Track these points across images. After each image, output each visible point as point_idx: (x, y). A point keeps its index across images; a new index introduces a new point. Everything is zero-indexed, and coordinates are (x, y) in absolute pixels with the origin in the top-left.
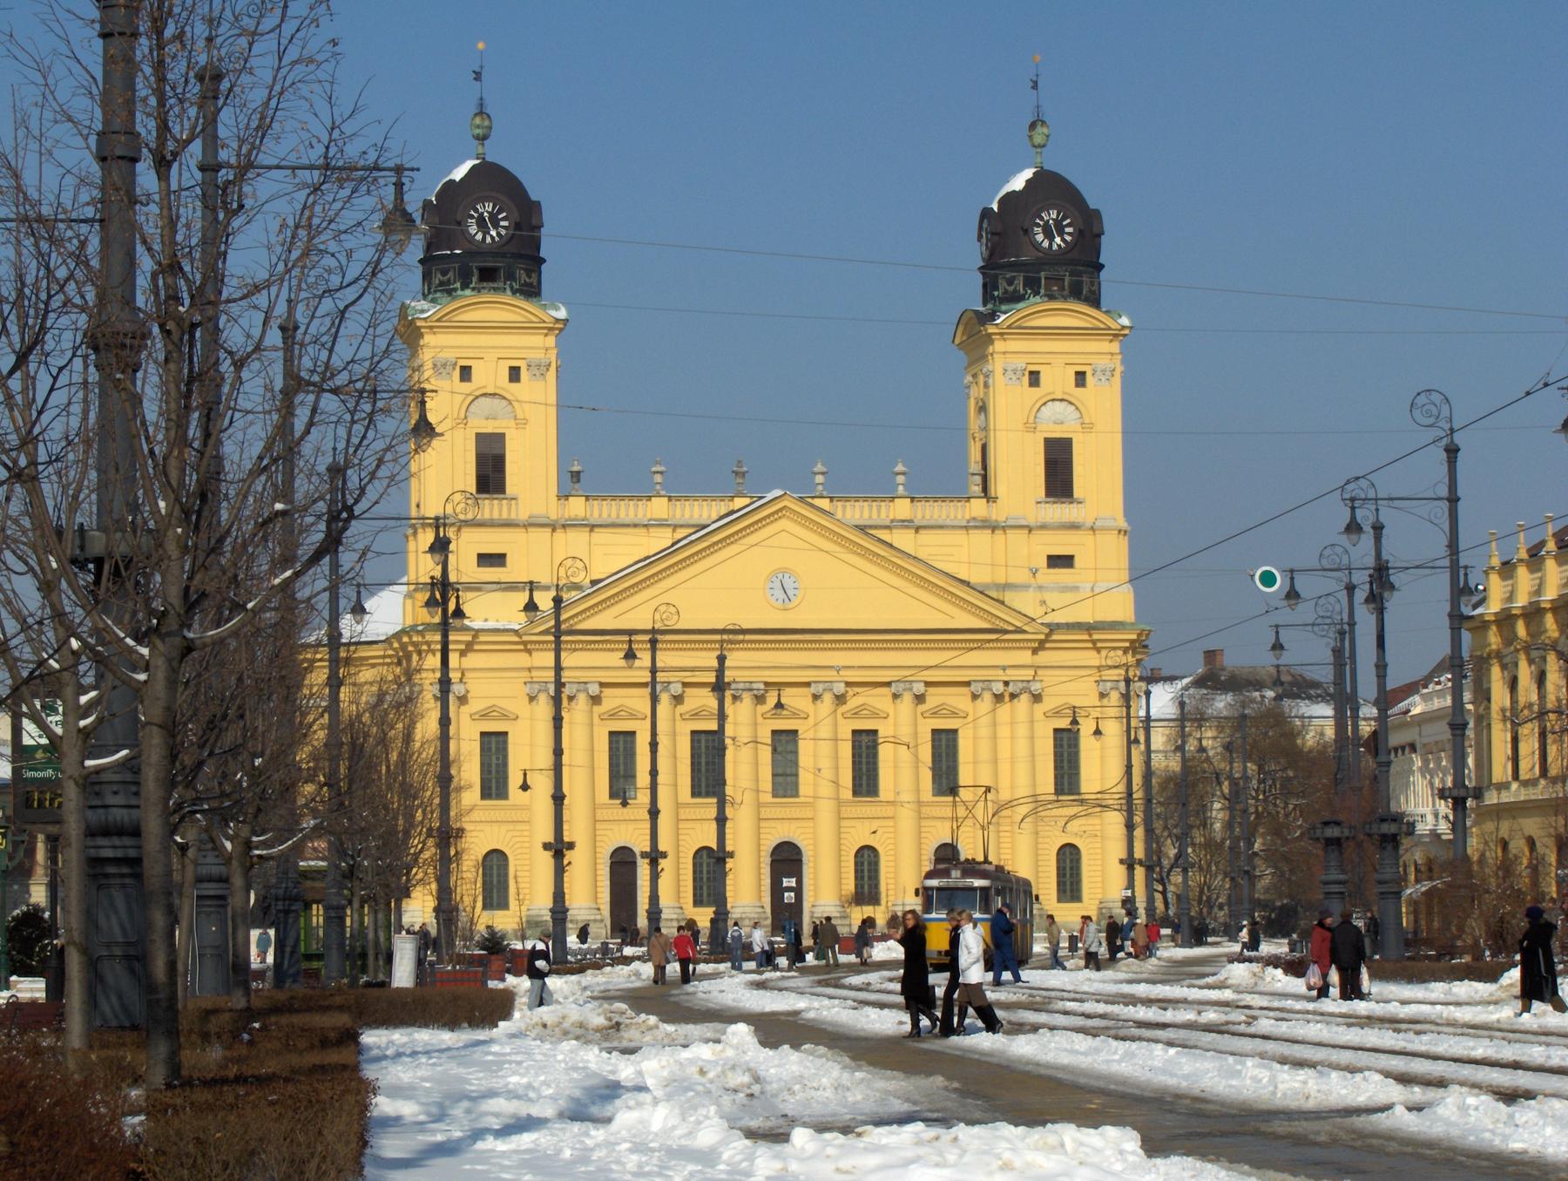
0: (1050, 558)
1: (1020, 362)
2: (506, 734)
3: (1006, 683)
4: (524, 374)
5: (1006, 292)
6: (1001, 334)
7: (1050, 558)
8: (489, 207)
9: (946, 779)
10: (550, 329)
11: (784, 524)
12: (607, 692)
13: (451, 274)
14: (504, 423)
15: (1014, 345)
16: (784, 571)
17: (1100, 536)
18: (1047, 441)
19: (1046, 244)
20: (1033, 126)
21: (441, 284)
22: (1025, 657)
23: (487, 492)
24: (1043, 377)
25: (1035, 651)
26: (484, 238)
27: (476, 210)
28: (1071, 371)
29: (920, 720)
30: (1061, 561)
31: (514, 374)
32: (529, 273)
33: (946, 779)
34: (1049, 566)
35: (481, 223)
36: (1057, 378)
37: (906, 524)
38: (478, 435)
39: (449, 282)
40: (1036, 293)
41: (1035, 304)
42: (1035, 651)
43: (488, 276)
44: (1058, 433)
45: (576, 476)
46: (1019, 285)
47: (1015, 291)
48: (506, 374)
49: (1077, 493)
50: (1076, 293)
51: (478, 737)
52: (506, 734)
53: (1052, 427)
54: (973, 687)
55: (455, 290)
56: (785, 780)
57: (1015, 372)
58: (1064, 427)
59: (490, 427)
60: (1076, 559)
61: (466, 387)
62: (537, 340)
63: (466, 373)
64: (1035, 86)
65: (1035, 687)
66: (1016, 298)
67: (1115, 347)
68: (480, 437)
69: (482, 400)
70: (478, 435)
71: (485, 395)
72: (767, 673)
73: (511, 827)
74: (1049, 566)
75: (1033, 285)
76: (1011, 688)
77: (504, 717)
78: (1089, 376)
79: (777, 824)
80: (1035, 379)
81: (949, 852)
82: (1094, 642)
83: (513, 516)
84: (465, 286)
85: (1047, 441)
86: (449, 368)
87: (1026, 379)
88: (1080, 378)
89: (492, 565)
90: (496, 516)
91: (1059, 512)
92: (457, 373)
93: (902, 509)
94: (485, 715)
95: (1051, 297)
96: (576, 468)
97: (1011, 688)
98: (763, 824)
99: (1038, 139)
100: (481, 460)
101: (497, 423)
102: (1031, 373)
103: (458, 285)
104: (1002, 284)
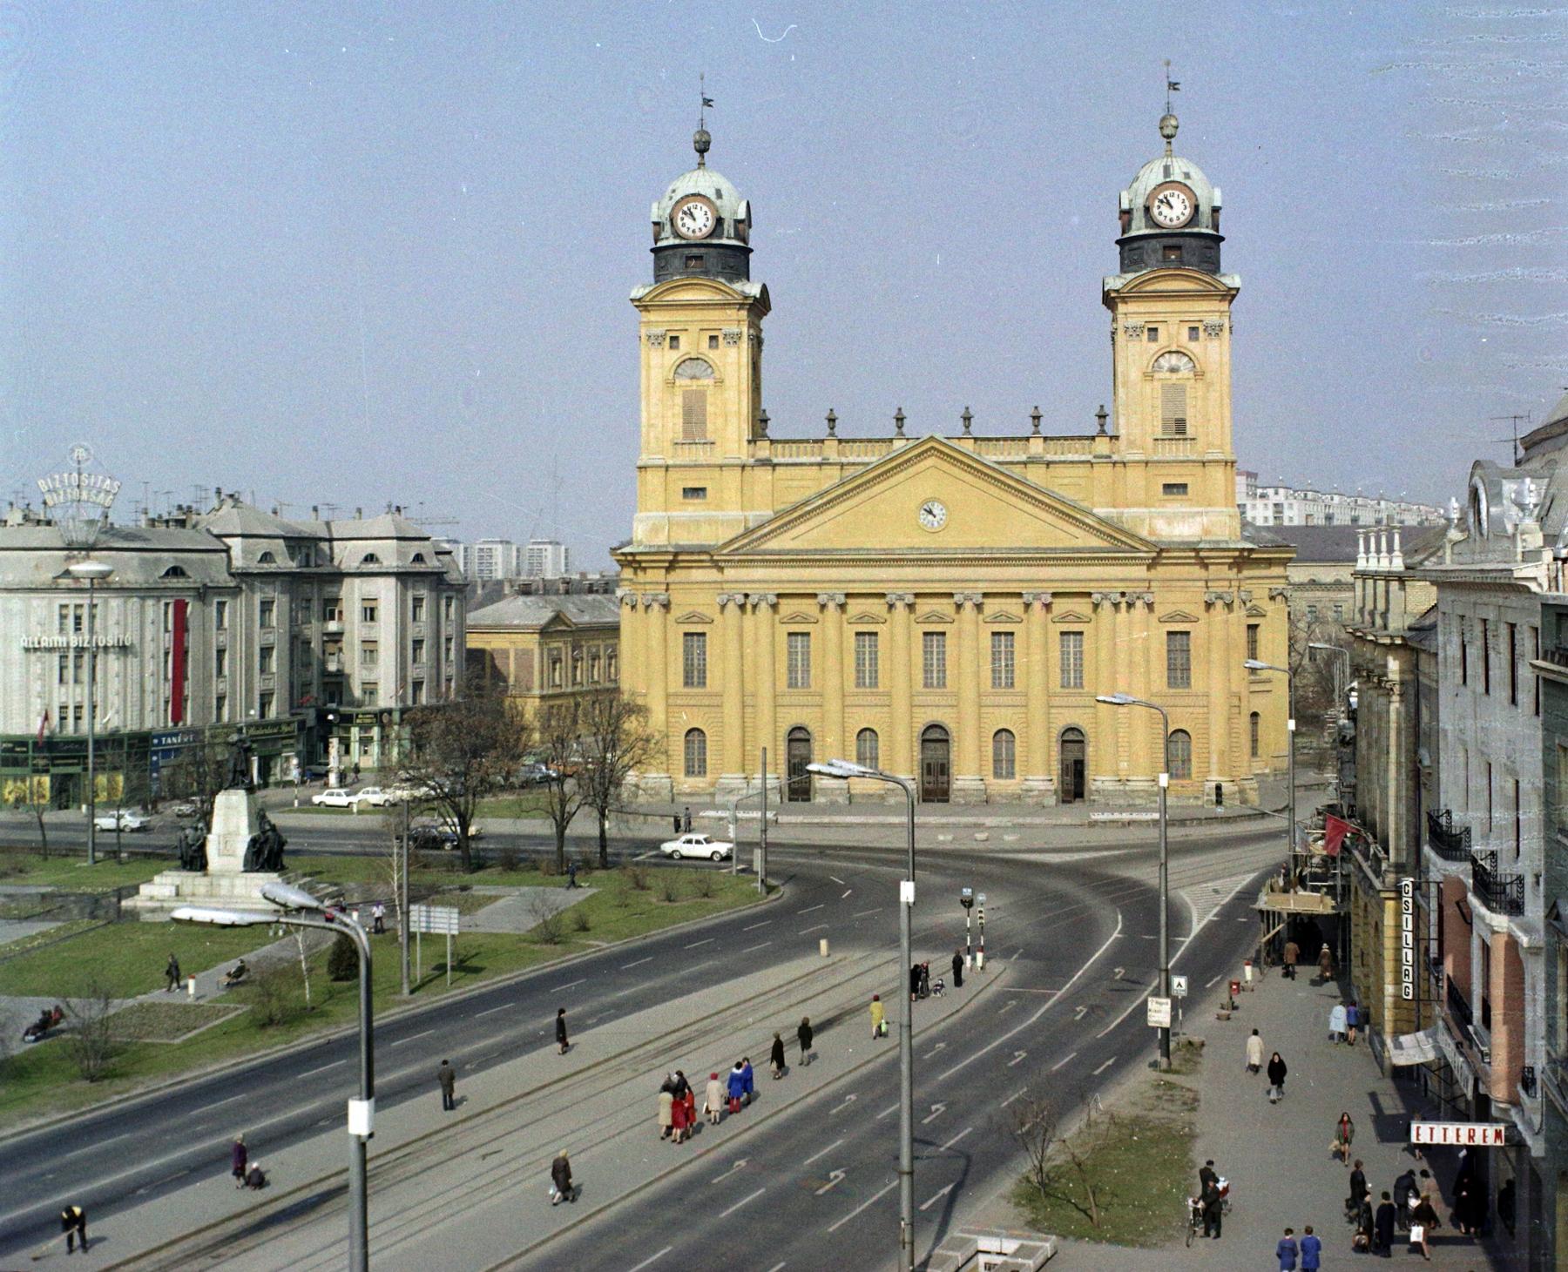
3: (1123, 594)
11: (931, 461)
12: (783, 601)
15: (1132, 307)
17: (1210, 469)
20: (1163, 119)
22: (1140, 572)
25: (1150, 567)
29: (1051, 625)
36: (1174, 333)
42: (1150, 567)
53: (1168, 375)
54: (956, 598)
57: (1135, 328)
58: (1180, 375)
59: (694, 385)
62: (732, 313)
65: (1148, 598)
67: (1224, 306)
76: (1119, 599)
78: (1201, 334)
87: (1145, 336)
97: (1119, 599)
98: (915, 710)
99: (1168, 131)
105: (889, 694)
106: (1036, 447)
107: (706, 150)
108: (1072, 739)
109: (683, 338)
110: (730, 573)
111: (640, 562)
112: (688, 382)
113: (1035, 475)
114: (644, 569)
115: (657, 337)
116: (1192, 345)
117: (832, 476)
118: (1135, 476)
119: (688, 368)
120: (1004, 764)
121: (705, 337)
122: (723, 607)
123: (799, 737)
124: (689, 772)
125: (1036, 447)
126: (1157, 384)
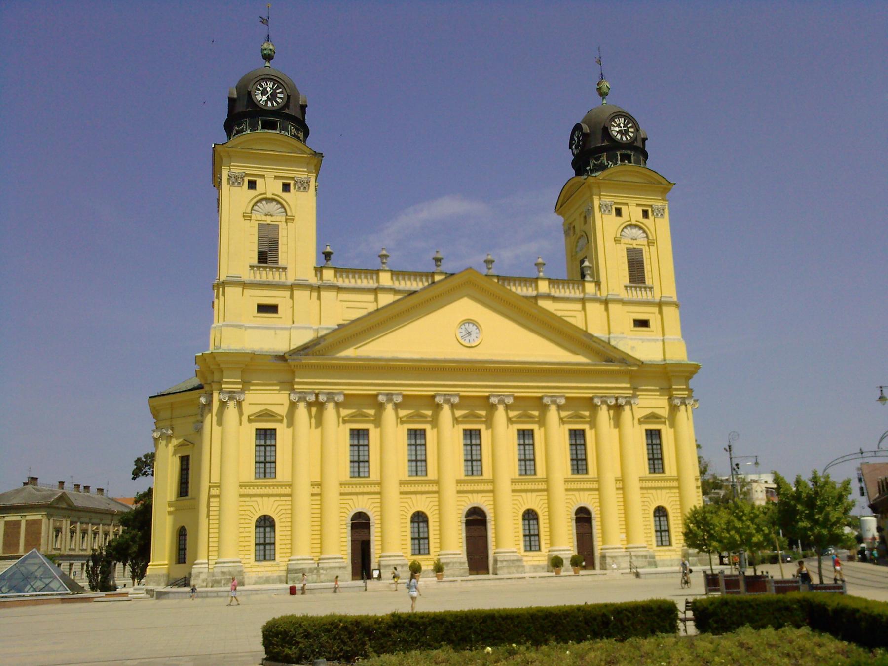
2: (275, 430)
13: (244, 126)
16: (469, 321)
18: (628, 250)
19: (619, 136)
24: (624, 209)
27: (262, 86)
30: (643, 323)
31: (286, 187)
32: (297, 130)
33: (579, 463)
36: (632, 212)
43: (269, 125)
45: (327, 255)
46: (604, 159)
49: (648, 282)
50: (638, 162)
52: (275, 430)
53: (631, 241)
59: (269, 220)
60: (651, 323)
61: (252, 193)
63: (252, 185)
64: (599, 62)
66: (603, 168)
68: (261, 227)
71: (266, 199)
73: (278, 498)
75: (612, 158)
79: (470, 495)
80: (619, 212)
83: (283, 279)
86: (240, 180)
88: (645, 214)
96: (328, 249)
99: (605, 90)
101: (273, 218)
104: (593, 162)
105: (437, 482)
106: (543, 287)
109: (259, 181)
112: (264, 218)
113: (544, 304)
115: (236, 178)
116: (645, 221)
117: (386, 299)
119: (264, 206)
120: (532, 540)
121: (279, 183)
123: (360, 524)
125: (543, 287)
126: (624, 247)
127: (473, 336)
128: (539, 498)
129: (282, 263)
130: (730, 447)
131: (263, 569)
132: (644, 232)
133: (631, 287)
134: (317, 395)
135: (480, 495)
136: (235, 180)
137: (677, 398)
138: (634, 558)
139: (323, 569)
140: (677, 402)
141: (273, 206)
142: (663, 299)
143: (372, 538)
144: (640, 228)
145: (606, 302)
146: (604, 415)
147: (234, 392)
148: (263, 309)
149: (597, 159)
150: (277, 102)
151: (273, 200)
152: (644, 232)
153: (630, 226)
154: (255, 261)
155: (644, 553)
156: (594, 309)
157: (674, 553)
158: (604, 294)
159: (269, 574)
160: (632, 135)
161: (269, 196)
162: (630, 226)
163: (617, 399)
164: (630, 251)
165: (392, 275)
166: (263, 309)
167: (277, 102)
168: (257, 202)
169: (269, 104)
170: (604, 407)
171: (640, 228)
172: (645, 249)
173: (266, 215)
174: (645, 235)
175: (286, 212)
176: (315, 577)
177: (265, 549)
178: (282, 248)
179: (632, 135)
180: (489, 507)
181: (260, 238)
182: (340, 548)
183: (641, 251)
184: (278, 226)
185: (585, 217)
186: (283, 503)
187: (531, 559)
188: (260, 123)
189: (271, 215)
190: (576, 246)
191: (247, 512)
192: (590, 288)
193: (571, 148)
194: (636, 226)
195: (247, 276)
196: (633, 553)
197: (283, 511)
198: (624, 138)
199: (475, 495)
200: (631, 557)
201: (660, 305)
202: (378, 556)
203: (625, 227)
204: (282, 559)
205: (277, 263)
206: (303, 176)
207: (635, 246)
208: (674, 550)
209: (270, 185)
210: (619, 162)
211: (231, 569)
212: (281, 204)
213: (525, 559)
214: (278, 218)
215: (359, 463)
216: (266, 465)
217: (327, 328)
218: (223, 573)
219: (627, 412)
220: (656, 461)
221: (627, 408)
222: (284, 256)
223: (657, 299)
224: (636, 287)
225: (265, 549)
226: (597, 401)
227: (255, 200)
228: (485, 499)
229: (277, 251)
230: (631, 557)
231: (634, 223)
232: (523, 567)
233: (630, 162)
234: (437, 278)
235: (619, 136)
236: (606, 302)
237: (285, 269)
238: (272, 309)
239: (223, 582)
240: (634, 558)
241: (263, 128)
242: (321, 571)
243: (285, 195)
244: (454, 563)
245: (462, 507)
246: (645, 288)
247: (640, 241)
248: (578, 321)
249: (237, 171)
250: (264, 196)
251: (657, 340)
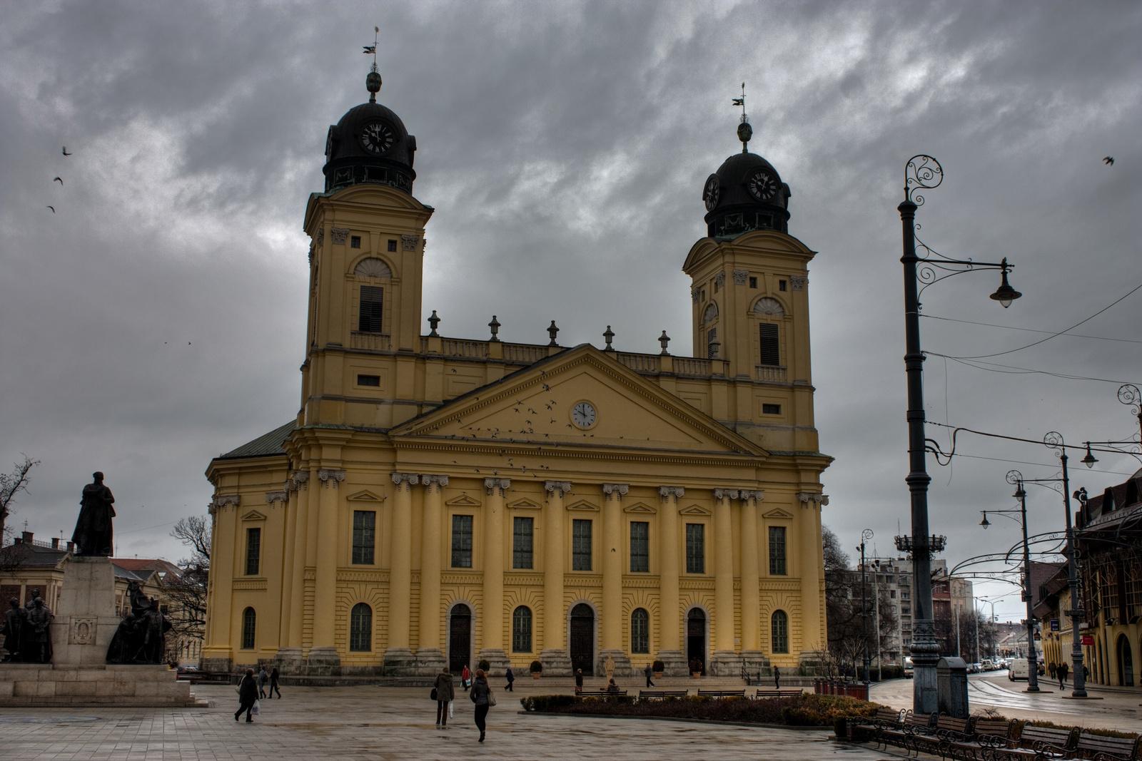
0: (765, 405)
1: (743, 269)
4: (399, 247)
5: (730, 224)
6: (732, 249)
7: (765, 405)
8: (377, 129)
9: (695, 561)
10: (421, 214)
13: (348, 173)
14: (383, 280)
16: (584, 403)
18: (761, 325)
19: (759, 195)
21: (340, 181)
22: (750, 474)
23: (368, 330)
24: (760, 282)
26: (374, 149)
28: (777, 279)
30: (772, 409)
31: (392, 245)
33: (695, 561)
34: (764, 412)
35: (373, 140)
36: (769, 283)
37: (672, 375)
38: (362, 287)
39: (346, 179)
40: (753, 226)
41: (752, 233)
42: (758, 469)
43: (376, 176)
44: (769, 320)
47: (738, 225)
48: (385, 245)
51: (352, 514)
53: (765, 316)
55: (352, 183)
56: (583, 558)
59: (372, 283)
60: (782, 409)
61: (355, 252)
63: (356, 241)
66: (737, 230)
69: (368, 261)
70: (362, 287)
72: (571, 476)
73: (376, 586)
74: (764, 412)
77: (372, 498)
78: (788, 286)
80: (753, 282)
81: (698, 616)
82: (796, 465)
84: (358, 181)
85: (761, 325)
87: (748, 282)
88: (783, 285)
89: (367, 384)
90: (373, 348)
91: (769, 375)
92: (349, 241)
93: (666, 365)
94: (358, 498)
95: (760, 229)
99: (745, 136)
100: (364, 305)
101: (378, 280)
102: (751, 278)
103: (353, 180)
107: (377, 89)
108: (697, 621)
110: (402, 456)
111: (317, 439)
112: (368, 279)
114: (320, 447)
116: (782, 294)
118: (744, 392)
122: (396, 486)
124: (354, 647)
126: (758, 322)
127: (588, 420)
128: (650, 597)
129: (385, 330)
130: (863, 546)
131: (357, 659)
132: (781, 306)
133: (763, 367)
134: (420, 477)
135: (588, 591)
136: (338, 236)
137: (805, 493)
138: (747, 665)
139: (421, 662)
140: (804, 497)
141: (378, 267)
142: (796, 384)
143: (472, 632)
144: (777, 301)
145: (733, 383)
146: (725, 509)
147: (334, 471)
148: (366, 380)
149: (734, 219)
150: (385, 147)
151: (377, 259)
152: (781, 306)
153: (766, 298)
154: (357, 327)
155: (759, 660)
156: (720, 391)
157: (791, 661)
158: (732, 375)
159: (365, 664)
160: (772, 192)
161: (374, 255)
162: (766, 298)
163: (740, 492)
164: (763, 327)
165: (503, 346)
166: (366, 380)
167: (385, 147)
168: (359, 263)
169: (377, 150)
170: (726, 500)
171: (777, 301)
172: (780, 326)
173: (370, 276)
174: (780, 310)
175: (391, 273)
176: (413, 669)
177: (361, 639)
178: (385, 313)
179: (772, 192)
180: (596, 604)
181: (361, 301)
182: (436, 638)
183: (776, 327)
184: (382, 288)
185: (716, 284)
186: (382, 591)
187: (638, 661)
188: (367, 171)
189: (375, 276)
190: (705, 314)
191: (344, 599)
192: (717, 368)
193: (704, 199)
194: (772, 299)
195: (347, 344)
196: (746, 660)
197: (381, 600)
198: (764, 197)
199: (583, 591)
200: (744, 664)
201: (793, 388)
202: (477, 651)
203: (760, 300)
204: (378, 650)
205: (380, 331)
206: (411, 234)
207: (769, 322)
208: (792, 658)
209: (375, 243)
210: (757, 225)
211: (328, 658)
212: (386, 264)
213: (632, 661)
214: (383, 280)
215: (461, 552)
216: (363, 552)
217: (432, 405)
218: (320, 661)
219: (750, 510)
220: (777, 563)
221: (751, 502)
222: (388, 323)
223: (790, 381)
224: (768, 368)
225: (361, 639)
226: (718, 493)
227: (359, 260)
228: (593, 595)
229: (380, 315)
230: (744, 664)
231: (769, 295)
232: (630, 668)
233: (769, 225)
234: (552, 352)
235: (759, 195)
236: (733, 383)
237: (389, 337)
238: (372, 380)
239: (320, 670)
240: (747, 665)
241: (370, 176)
242: (420, 665)
243: (391, 255)
244: (557, 662)
245: (569, 604)
246: (778, 369)
247: (775, 319)
248: (701, 405)
249: (341, 227)
250: (369, 255)
251: (788, 428)
